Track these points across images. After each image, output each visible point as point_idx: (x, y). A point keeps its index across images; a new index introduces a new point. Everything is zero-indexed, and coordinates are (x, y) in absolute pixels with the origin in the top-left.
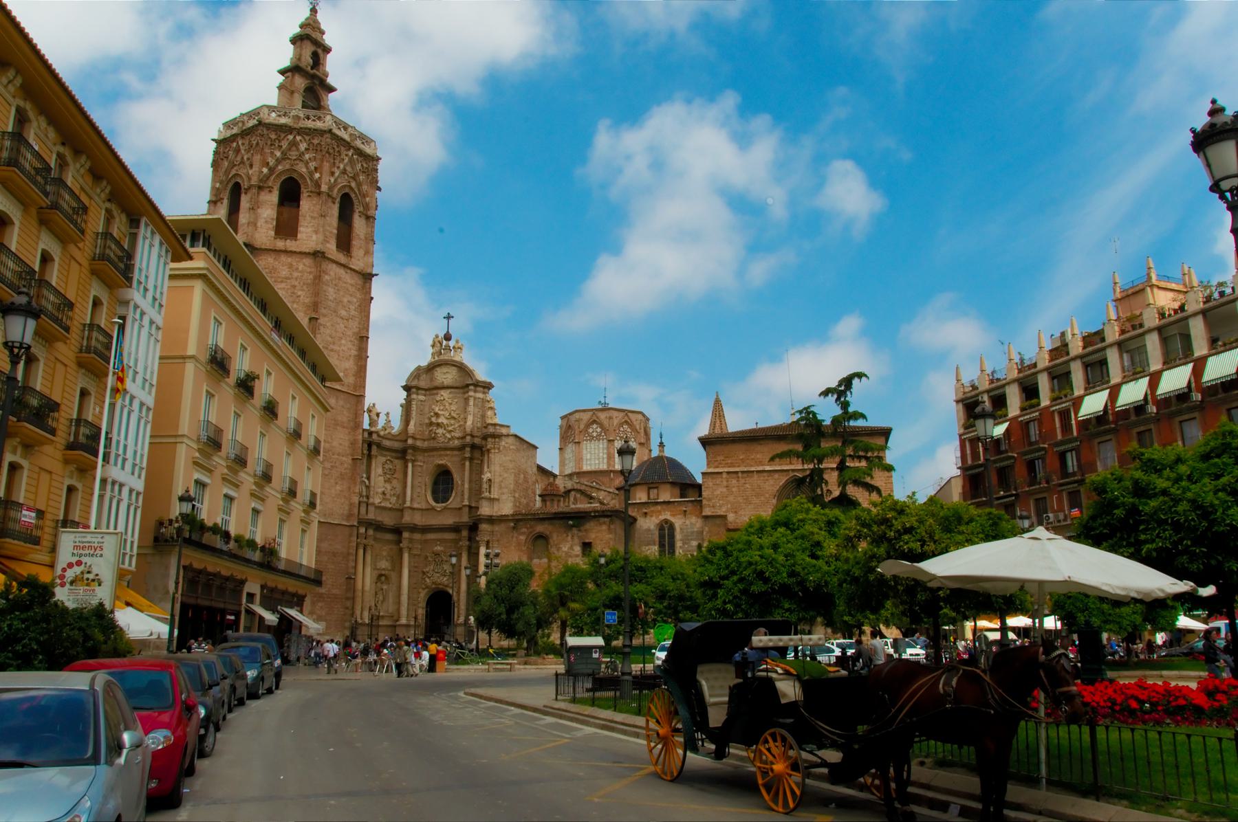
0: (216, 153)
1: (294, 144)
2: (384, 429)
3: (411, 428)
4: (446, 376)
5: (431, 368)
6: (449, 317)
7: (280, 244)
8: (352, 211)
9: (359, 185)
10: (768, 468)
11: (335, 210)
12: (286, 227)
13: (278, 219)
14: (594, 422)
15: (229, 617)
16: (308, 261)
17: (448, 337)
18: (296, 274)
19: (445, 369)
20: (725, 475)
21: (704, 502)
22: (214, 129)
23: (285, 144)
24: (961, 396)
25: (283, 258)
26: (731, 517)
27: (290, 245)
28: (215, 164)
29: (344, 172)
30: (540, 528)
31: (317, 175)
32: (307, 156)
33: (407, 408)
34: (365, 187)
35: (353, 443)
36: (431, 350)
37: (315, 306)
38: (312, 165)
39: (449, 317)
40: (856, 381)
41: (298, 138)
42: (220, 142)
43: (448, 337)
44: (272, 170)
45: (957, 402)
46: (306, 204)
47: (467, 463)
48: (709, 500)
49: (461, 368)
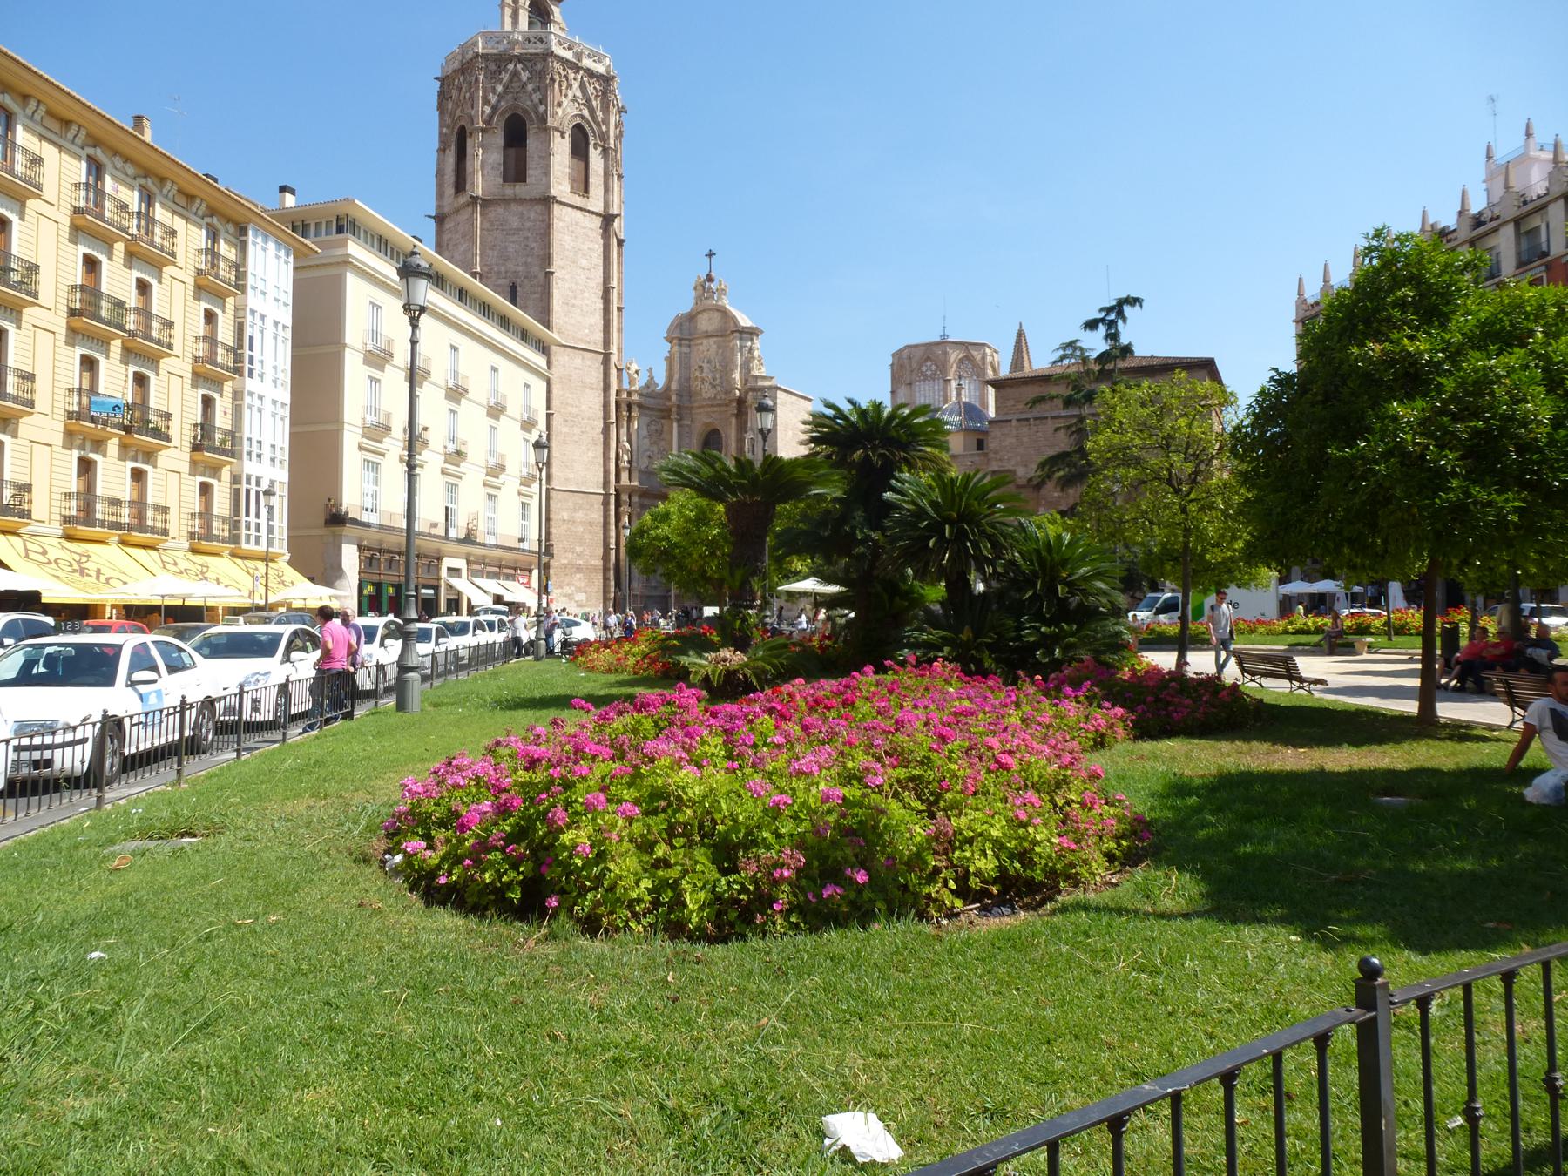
0: (443, 96)
1: (515, 74)
2: (647, 386)
3: (674, 386)
5: (691, 318)
6: (710, 255)
7: (509, 191)
8: (587, 144)
9: (592, 111)
10: (1063, 413)
12: (515, 170)
13: (504, 163)
14: (928, 358)
15: (424, 591)
16: (539, 208)
17: (710, 279)
18: (528, 224)
19: (705, 316)
20: (1014, 423)
21: (992, 455)
22: (435, 67)
23: (505, 77)
24: (1302, 315)
25: (514, 207)
26: (1021, 471)
27: (519, 190)
28: (441, 107)
29: (574, 99)
31: (542, 108)
32: (530, 87)
33: (670, 360)
34: (600, 114)
35: (606, 406)
36: (693, 294)
37: (547, 259)
38: (536, 97)
39: (710, 255)
40: (1127, 309)
41: (519, 66)
42: (442, 80)
43: (710, 279)
44: (495, 108)
45: (1297, 322)
46: (532, 143)
47: (734, 420)
48: (996, 452)
49: (724, 312)
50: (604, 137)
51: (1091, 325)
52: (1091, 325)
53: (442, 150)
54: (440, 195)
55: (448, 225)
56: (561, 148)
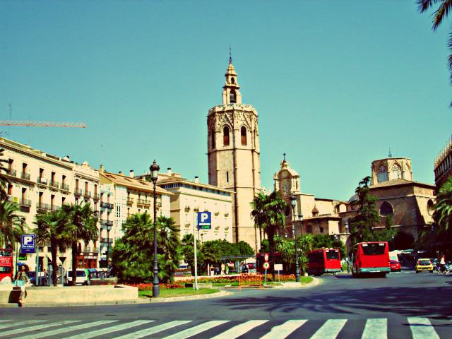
0: (208, 120)
4: (284, 175)
11: (240, 132)
12: (226, 142)
25: (226, 152)
28: (208, 124)
30: (310, 224)
37: (235, 165)
43: (284, 162)
50: (250, 128)
51: (362, 183)
52: (362, 183)
53: (209, 136)
54: (209, 148)
55: (211, 156)
56: (238, 134)
